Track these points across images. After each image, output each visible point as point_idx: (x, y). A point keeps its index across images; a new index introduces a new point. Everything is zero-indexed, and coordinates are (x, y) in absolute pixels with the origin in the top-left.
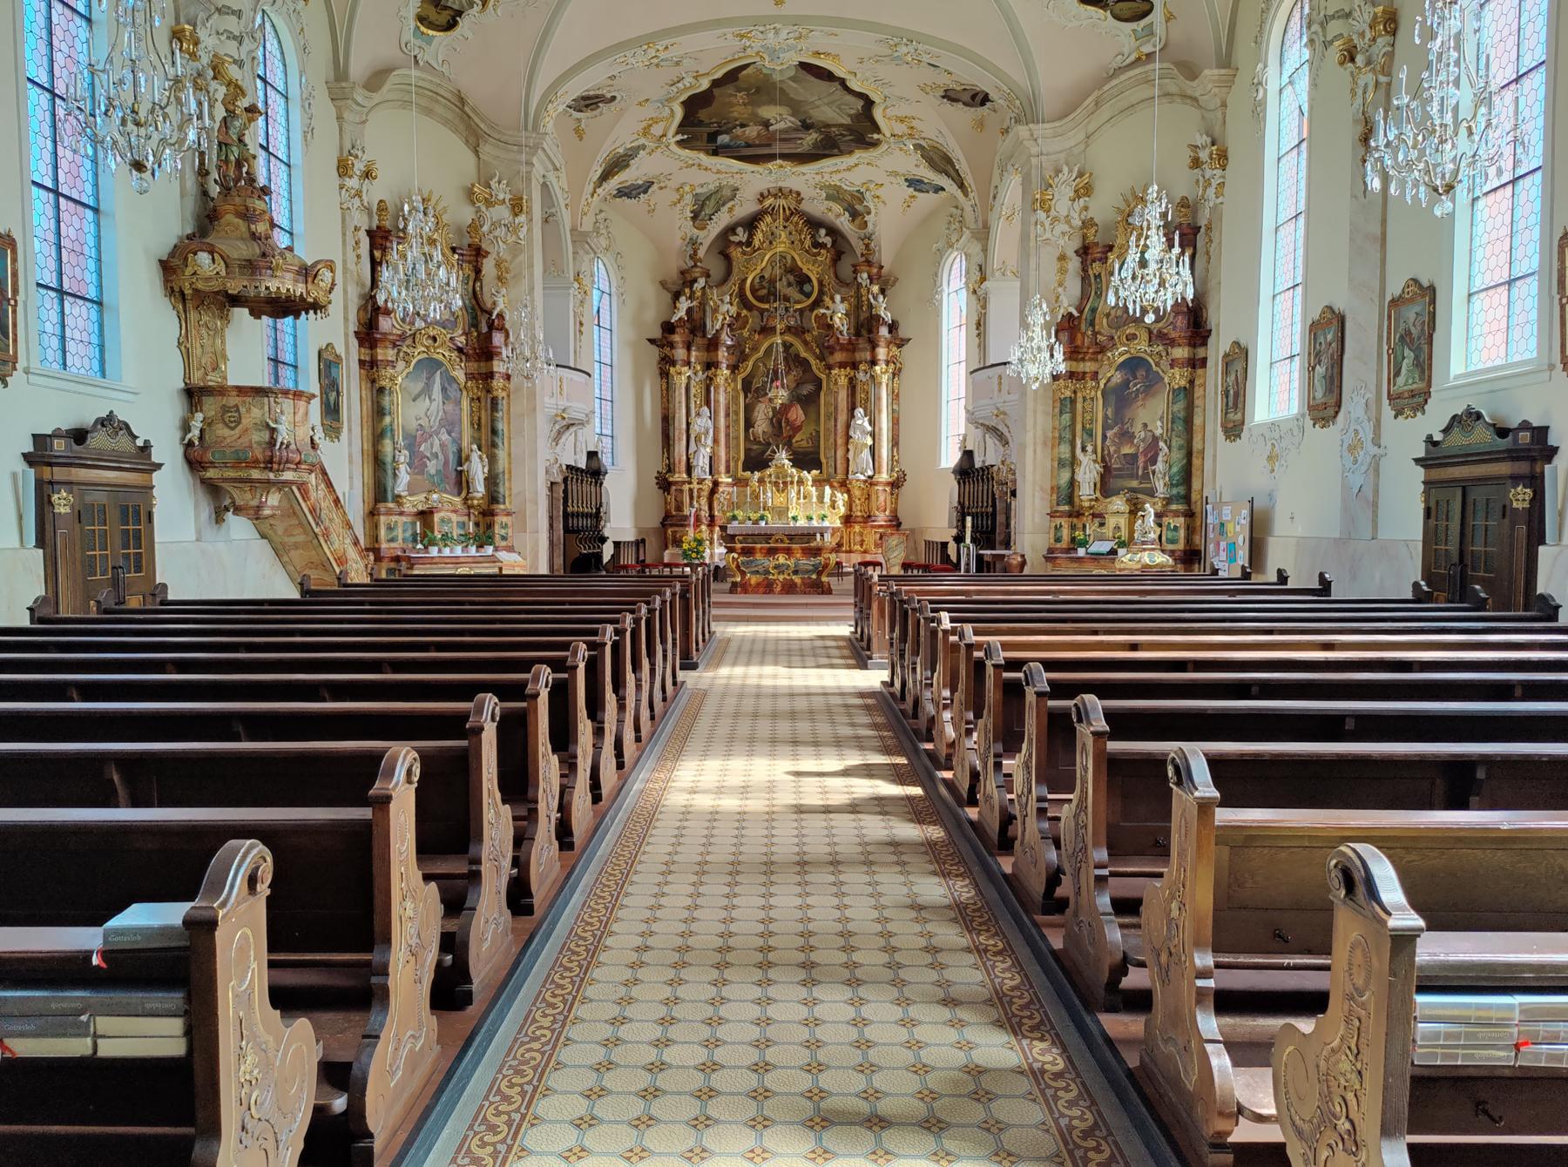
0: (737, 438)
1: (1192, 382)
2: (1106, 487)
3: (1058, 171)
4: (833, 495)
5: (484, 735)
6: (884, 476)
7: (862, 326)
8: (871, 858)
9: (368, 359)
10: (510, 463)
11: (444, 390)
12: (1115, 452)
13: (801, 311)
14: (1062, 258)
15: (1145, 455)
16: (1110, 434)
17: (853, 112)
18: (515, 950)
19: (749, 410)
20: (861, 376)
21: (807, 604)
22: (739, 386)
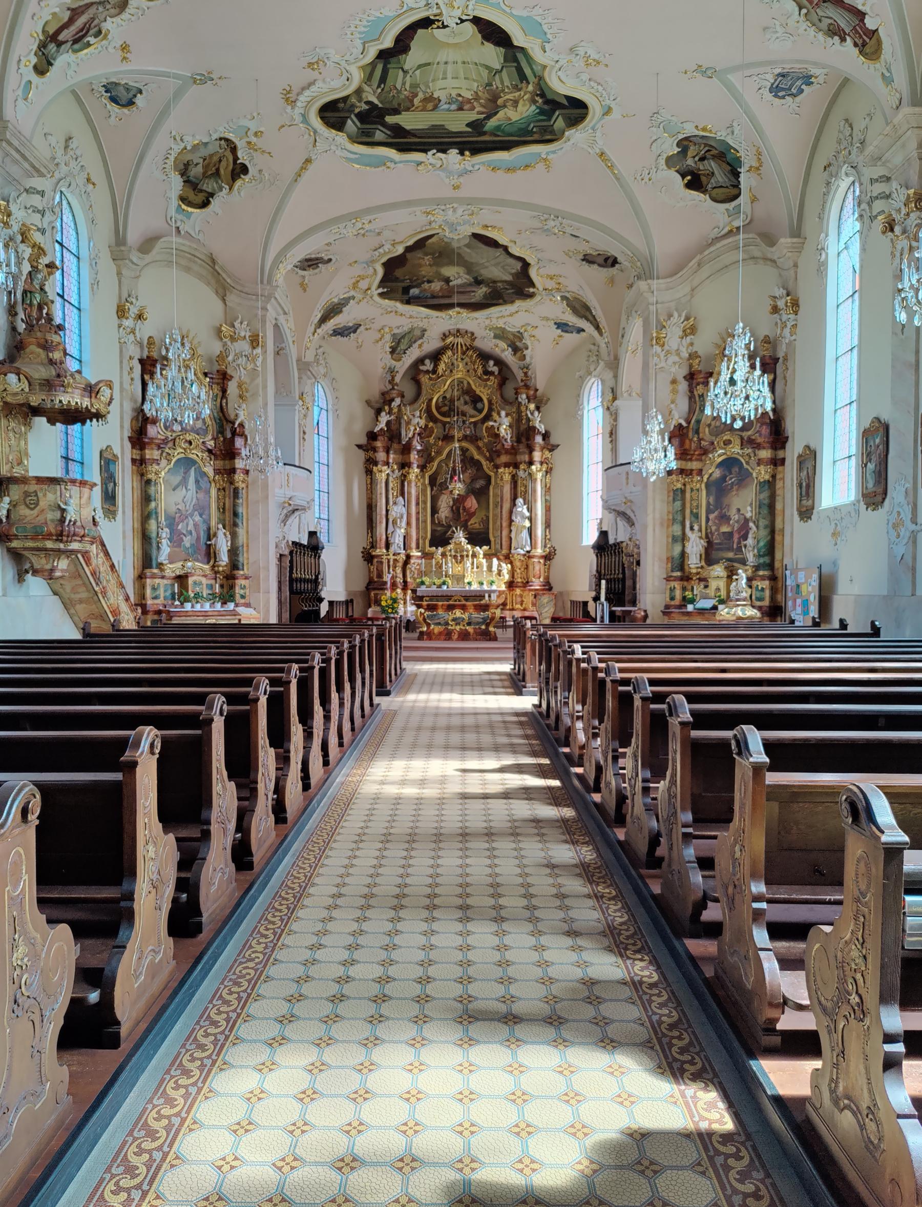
0: (425, 522)
1: (774, 476)
2: (709, 558)
3: (670, 316)
4: (499, 565)
5: (214, 725)
6: (539, 551)
7: (522, 435)
8: (518, 831)
9: (138, 458)
10: (247, 539)
11: (197, 482)
12: (716, 530)
13: (475, 423)
14: (674, 382)
15: (739, 533)
16: (712, 516)
17: (513, 271)
18: (237, 895)
19: (435, 500)
20: (521, 473)
21: (477, 648)
22: (427, 482)
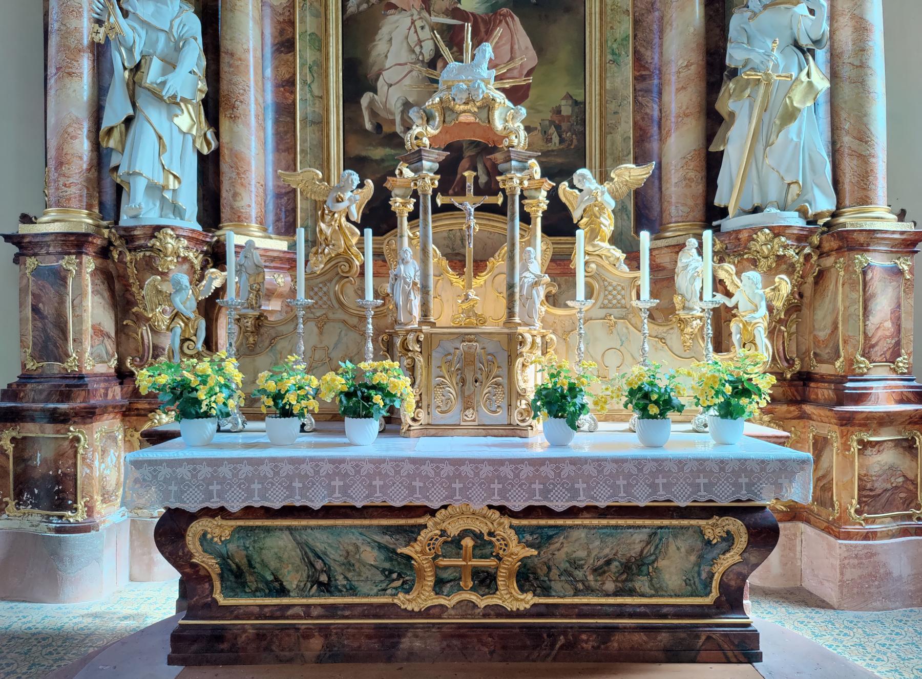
0: (321, 123)
